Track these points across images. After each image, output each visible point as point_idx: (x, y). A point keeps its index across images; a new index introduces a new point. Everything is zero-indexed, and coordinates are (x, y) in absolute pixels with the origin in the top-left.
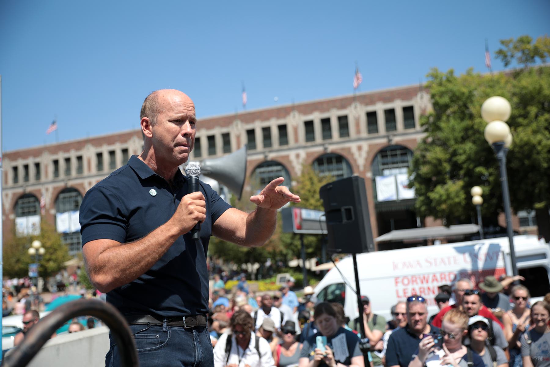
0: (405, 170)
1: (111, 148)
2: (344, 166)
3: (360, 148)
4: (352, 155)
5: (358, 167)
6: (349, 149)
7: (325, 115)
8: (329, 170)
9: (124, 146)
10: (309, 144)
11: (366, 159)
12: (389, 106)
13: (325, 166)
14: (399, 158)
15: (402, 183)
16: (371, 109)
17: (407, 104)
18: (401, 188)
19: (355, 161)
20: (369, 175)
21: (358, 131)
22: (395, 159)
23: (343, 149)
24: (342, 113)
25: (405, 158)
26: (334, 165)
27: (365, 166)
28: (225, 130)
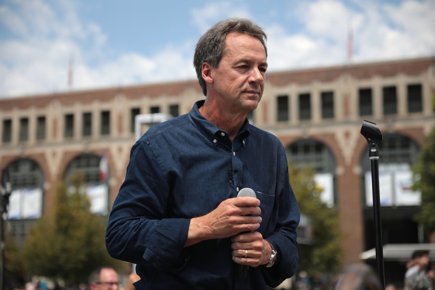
0: (405, 167)
1: (24, 114)
2: (325, 155)
3: (347, 135)
4: (336, 143)
5: (343, 159)
6: (332, 136)
7: (304, 89)
8: (307, 161)
9: (41, 112)
10: (282, 125)
11: (355, 150)
12: (389, 82)
13: (301, 156)
14: (398, 151)
15: (401, 184)
16: (365, 84)
17: (413, 80)
18: (399, 191)
19: (340, 151)
20: (357, 170)
21: (346, 112)
22: (393, 152)
23: (326, 135)
24: (327, 87)
25: (405, 151)
26: (312, 156)
27: (353, 158)
28: (173, 100)
